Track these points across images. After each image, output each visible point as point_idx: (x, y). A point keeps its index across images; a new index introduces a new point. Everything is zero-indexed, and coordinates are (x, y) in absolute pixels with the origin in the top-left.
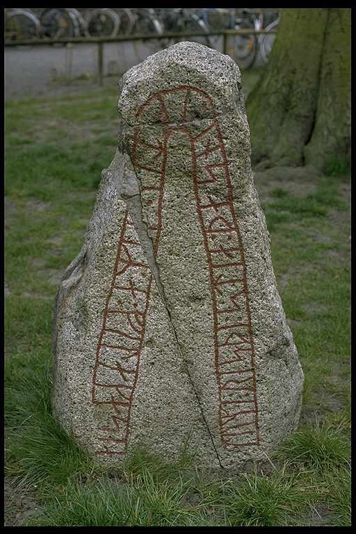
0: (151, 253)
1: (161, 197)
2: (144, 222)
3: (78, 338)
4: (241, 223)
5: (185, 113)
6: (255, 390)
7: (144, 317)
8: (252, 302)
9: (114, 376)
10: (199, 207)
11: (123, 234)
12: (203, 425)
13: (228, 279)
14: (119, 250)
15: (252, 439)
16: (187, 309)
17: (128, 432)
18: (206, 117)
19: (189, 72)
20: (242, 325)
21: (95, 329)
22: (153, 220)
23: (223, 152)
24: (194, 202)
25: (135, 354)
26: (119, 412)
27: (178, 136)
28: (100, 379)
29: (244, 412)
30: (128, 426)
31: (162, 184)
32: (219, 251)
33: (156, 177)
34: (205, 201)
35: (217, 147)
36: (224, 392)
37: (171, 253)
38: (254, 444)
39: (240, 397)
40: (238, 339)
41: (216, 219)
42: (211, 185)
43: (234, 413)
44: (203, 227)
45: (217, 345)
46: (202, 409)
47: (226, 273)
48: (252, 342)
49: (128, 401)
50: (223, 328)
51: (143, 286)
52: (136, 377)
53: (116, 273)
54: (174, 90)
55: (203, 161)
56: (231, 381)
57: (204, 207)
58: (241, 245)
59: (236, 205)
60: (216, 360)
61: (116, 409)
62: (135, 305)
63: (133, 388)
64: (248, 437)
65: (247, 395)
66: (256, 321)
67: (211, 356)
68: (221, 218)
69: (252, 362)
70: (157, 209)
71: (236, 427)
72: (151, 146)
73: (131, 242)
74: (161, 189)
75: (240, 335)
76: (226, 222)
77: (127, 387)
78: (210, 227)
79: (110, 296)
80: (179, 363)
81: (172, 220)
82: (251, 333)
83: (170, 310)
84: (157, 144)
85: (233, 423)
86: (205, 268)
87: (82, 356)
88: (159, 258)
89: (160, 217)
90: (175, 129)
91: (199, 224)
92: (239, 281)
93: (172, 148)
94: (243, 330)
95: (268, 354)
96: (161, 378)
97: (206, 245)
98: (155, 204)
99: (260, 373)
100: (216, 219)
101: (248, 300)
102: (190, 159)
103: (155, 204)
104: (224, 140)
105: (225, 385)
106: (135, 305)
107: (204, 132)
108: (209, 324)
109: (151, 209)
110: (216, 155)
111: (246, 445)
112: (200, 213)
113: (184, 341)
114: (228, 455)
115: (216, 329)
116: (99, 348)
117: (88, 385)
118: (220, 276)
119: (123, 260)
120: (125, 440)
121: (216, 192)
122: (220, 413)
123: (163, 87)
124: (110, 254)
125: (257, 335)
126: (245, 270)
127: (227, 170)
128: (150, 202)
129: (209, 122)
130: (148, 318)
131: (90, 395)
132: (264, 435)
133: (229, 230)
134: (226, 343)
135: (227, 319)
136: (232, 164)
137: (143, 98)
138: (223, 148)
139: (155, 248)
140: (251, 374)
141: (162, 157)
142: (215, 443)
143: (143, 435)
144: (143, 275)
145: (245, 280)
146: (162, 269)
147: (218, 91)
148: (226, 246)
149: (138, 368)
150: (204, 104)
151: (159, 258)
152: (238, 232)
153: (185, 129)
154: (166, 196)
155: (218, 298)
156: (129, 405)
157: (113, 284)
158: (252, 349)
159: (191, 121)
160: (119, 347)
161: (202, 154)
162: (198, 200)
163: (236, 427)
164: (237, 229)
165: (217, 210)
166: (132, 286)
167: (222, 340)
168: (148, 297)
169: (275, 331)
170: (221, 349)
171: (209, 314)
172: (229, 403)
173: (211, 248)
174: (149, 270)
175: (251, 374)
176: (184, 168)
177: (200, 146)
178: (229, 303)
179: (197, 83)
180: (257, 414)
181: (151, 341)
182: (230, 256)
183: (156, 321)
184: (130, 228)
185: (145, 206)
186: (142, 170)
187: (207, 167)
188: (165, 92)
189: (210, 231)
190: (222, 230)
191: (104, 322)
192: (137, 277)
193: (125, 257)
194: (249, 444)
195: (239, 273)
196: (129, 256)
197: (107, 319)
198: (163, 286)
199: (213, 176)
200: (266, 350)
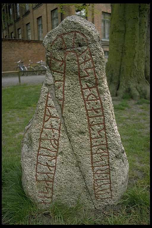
0: (60, 112)
2: (56, 97)
3: (28, 151)
6: (110, 174)
8: (108, 134)
9: (45, 168)
10: (82, 89)
11: (47, 103)
12: (87, 190)
13: (96, 123)
14: (46, 110)
15: (109, 196)
16: (77, 137)
17: (53, 194)
19: (75, 24)
20: (103, 144)
21: (36, 148)
22: (60, 96)
23: (93, 62)
24: (79, 87)
25: (54, 159)
26: (48, 185)
27: (71, 55)
28: (39, 170)
29: (105, 184)
30: (52, 191)
31: (64, 79)
33: (61, 76)
34: (84, 86)
36: (96, 175)
37: (69, 111)
38: (110, 198)
40: (101, 151)
41: (90, 95)
42: (87, 78)
43: (100, 184)
44: (84, 99)
45: (92, 154)
46: (86, 183)
47: (95, 121)
48: (108, 152)
49: (52, 180)
50: (95, 146)
51: (57, 127)
52: (55, 169)
53: (45, 121)
54: (68, 33)
56: (99, 170)
57: (84, 89)
58: (102, 107)
59: (99, 87)
61: (47, 183)
62: (54, 136)
63: (54, 174)
64: (107, 195)
65: (106, 176)
66: (110, 142)
67: (89, 159)
68: (92, 94)
69: (108, 161)
71: (101, 191)
72: (58, 60)
73: (50, 107)
74: (64, 81)
75: (102, 149)
77: (51, 174)
78: (87, 99)
79: (42, 132)
80: (75, 163)
82: (108, 148)
84: (61, 59)
85: (100, 189)
86: (86, 118)
87: (30, 160)
88: (64, 114)
90: (69, 52)
91: (82, 97)
92: (101, 124)
93: (68, 60)
95: (115, 158)
96: (67, 169)
97: (86, 107)
99: (112, 166)
100: (90, 95)
101: (106, 133)
103: (61, 89)
104: (93, 56)
105: (96, 172)
106: (54, 136)
107: (83, 52)
108: (88, 144)
109: (59, 91)
111: (106, 198)
112: (82, 92)
113: (77, 152)
114: (98, 203)
115: (91, 147)
116: (38, 156)
117: (34, 173)
118: (93, 122)
119: (47, 115)
120: (51, 197)
121: (89, 81)
122: (94, 185)
125: (110, 149)
126: (104, 118)
127: (95, 71)
128: (59, 87)
129: (85, 48)
130: (60, 142)
131: (35, 177)
132: (114, 194)
134: (96, 153)
135: (96, 142)
136: (97, 67)
138: (92, 60)
140: (108, 167)
141: (64, 66)
142: (92, 198)
143: (60, 195)
144: (57, 122)
145: (104, 124)
146: (65, 119)
148: (95, 108)
149: (56, 165)
150: (83, 39)
151: (64, 114)
152: (101, 101)
153: (74, 51)
155: (92, 132)
156: (53, 182)
157: (43, 127)
158: (108, 155)
160: (47, 156)
161: (82, 63)
162: (81, 86)
163: (101, 191)
164: (100, 99)
165: (90, 91)
166: (52, 127)
167: (94, 151)
168: (60, 132)
169: (119, 147)
171: (88, 140)
172: (98, 180)
173: (88, 109)
174: (59, 120)
175: (108, 167)
176: (74, 70)
177: (81, 59)
179: (79, 29)
180: (111, 185)
181: (61, 153)
182: (97, 112)
183: (64, 143)
184: (50, 100)
185: (57, 89)
186: (55, 73)
188: (64, 34)
189: (87, 100)
190: (93, 100)
191: (40, 144)
193: (48, 114)
194: (107, 198)
195: (101, 120)
196: (50, 113)
197: (41, 143)
198: (66, 127)
199: (88, 73)
200: (115, 156)
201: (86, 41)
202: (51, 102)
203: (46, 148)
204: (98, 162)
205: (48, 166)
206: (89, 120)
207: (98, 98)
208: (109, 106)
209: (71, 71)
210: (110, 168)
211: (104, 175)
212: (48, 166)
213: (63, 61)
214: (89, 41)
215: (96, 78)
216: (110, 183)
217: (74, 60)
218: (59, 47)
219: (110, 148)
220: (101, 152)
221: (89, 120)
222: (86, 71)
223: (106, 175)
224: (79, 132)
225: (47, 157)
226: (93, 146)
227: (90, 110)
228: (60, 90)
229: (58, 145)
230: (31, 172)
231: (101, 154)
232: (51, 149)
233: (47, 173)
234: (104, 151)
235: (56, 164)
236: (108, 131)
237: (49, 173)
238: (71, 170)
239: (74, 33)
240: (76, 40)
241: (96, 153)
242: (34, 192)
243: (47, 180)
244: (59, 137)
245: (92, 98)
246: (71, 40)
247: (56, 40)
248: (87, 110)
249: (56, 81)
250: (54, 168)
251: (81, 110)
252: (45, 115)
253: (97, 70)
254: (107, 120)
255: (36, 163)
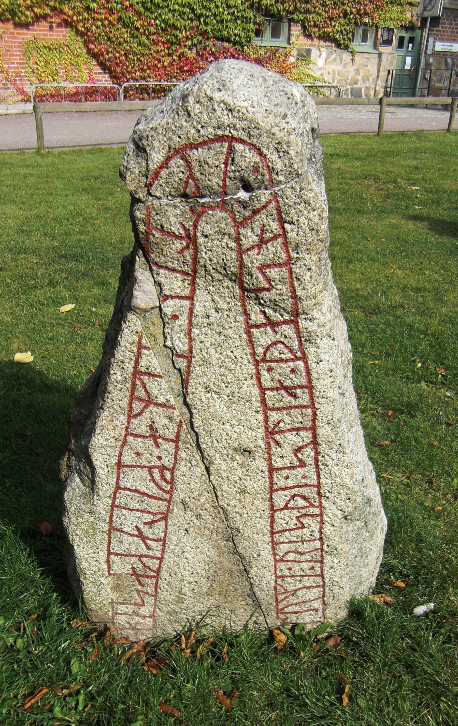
1: (191, 310)
4: (311, 350)
5: (224, 181)
6: (322, 562)
7: (172, 473)
10: (250, 327)
11: (137, 362)
13: (289, 427)
14: (134, 384)
18: (259, 188)
19: (231, 110)
20: (306, 485)
22: (181, 346)
23: (286, 244)
24: (241, 318)
27: (215, 222)
29: (308, 588)
30: (156, 600)
31: (193, 291)
32: (277, 389)
35: (276, 237)
36: (281, 565)
39: (303, 570)
40: (301, 502)
41: (275, 344)
42: (265, 295)
44: (254, 354)
45: (273, 509)
47: (287, 419)
48: (321, 506)
51: (171, 433)
52: (164, 545)
55: (254, 259)
57: (257, 326)
58: (310, 381)
59: (302, 323)
60: (272, 527)
61: (139, 581)
63: (161, 559)
64: (310, 615)
65: (312, 568)
68: (282, 343)
69: (320, 532)
70: (185, 328)
72: (173, 235)
73: (149, 374)
74: (191, 298)
75: (304, 498)
76: (287, 347)
77: (153, 558)
79: (123, 446)
81: (208, 344)
83: (207, 464)
84: (182, 231)
86: (257, 412)
89: (191, 340)
91: (248, 350)
92: (305, 429)
93: (206, 236)
94: (311, 492)
96: (197, 547)
97: (259, 379)
98: (183, 320)
100: (275, 344)
102: (234, 255)
104: (287, 226)
105: (283, 556)
107: (255, 212)
108: (259, 484)
109: (176, 328)
110: (274, 250)
115: (272, 491)
116: (112, 510)
117: (101, 553)
118: (279, 423)
121: (275, 305)
122: (275, 588)
123: (189, 138)
124: (121, 390)
125: (328, 498)
126: (315, 414)
128: (175, 317)
129: (264, 196)
130: (177, 473)
133: (292, 360)
134: (286, 507)
135: (287, 478)
136: (299, 263)
137: (157, 157)
138: (285, 237)
139: (184, 383)
140: (318, 544)
144: (171, 419)
145: (313, 429)
147: (279, 143)
148: (288, 383)
149: (165, 535)
150: (256, 169)
152: (306, 363)
153: (224, 205)
154: (198, 309)
158: (321, 515)
159: (235, 194)
160: (138, 510)
161: (253, 248)
164: (304, 358)
165: (275, 332)
166: (154, 435)
167: (279, 502)
168: (177, 447)
170: (278, 515)
172: (287, 576)
173: (267, 384)
177: (250, 237)
178: (290, 459)
182: (295, 397)
183: (190, 478)
186: (162, 271)
187: (262, 268)
188: (194, 146)
189: (264, 360)
190: (281, 360)
192: (162, 422)
195: (306, 418)
197: (122, 475)
199: (269, 280)
201: (266, 172)
202: (152, 360)
203: (136, 491)
204: (289, 530)
205: (144, 538)
206: (266, 418)
207: (299, 354)
208: (331, 377)
209: (213, 269)
210: (325, 547)
211: (305, 566)
212: (144, 538)
213: (188, 236)
214: (277, 174)
215: (294, 296)
216: (324, 586)
217: (226, 237)
218: (177, 189)
219: (328, 494)
220: (300, 506)
221: (266, 418)
222: (264, 274)
223: (311, 564)
224: (236, 450)
225: (138, 514)
226: (277, 490)
227: (272, 389)
228: (180, 326)
229: (172, 482)
230: (94, 553)
231: (301, 510)
232: (151, 494)
233: (140, 557)
234: (309, 502)
235: (165, 532)
236: (323, 448)
237: (145, 556)
238: (211, 549)
239: (226, 145)
240: (233, 168)
241: (286, 507)
242: (104, 602)
243: (139, 573)
244: (176, 459)
245: (280, 354)
246: (217, 166)
247: (165, 164)
248: (263, 390)
249: (167, 298)
250: (161, 543)
251: (245, 387)
252: (132, 397)
253: (298, 271)
254: (324, 418)
255: (107, 528)
